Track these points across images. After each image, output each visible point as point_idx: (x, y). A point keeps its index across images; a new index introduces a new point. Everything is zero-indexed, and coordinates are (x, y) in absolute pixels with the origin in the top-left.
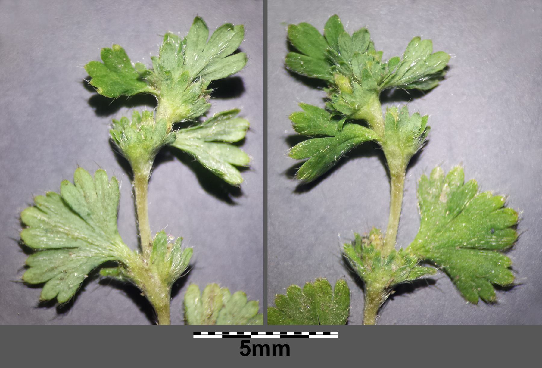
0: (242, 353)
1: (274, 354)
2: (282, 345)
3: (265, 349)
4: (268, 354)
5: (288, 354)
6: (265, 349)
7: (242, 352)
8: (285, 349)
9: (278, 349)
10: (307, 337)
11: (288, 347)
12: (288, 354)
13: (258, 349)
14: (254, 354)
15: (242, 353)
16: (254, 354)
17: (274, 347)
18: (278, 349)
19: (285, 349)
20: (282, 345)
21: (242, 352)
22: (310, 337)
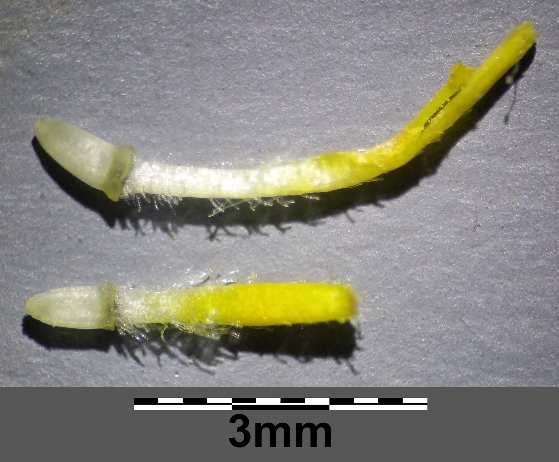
0: (233, 441)
1: (299, 443)
2: (316, 425)
3: (280, 432)
4: (287, 443)
5: (328, 443)
6: (280, 432)
7: (234, 438)
8: (321, 432)
9: (306, 433)
10: (326, 407)
11: (327, 427)
12: (328, 443)
13: (266, 433)
14: (259, 443)
15: (233, 441)
16: (259, 443)
17: (300, 428)
18: (306, 433)
19: (321, 432)
20: (316, 425)
21: (234, 438)
22: (333, 408)
